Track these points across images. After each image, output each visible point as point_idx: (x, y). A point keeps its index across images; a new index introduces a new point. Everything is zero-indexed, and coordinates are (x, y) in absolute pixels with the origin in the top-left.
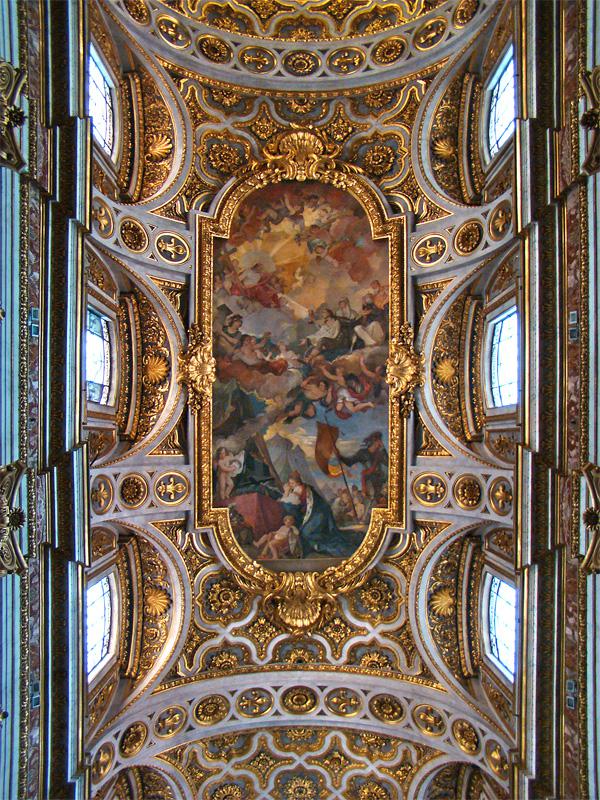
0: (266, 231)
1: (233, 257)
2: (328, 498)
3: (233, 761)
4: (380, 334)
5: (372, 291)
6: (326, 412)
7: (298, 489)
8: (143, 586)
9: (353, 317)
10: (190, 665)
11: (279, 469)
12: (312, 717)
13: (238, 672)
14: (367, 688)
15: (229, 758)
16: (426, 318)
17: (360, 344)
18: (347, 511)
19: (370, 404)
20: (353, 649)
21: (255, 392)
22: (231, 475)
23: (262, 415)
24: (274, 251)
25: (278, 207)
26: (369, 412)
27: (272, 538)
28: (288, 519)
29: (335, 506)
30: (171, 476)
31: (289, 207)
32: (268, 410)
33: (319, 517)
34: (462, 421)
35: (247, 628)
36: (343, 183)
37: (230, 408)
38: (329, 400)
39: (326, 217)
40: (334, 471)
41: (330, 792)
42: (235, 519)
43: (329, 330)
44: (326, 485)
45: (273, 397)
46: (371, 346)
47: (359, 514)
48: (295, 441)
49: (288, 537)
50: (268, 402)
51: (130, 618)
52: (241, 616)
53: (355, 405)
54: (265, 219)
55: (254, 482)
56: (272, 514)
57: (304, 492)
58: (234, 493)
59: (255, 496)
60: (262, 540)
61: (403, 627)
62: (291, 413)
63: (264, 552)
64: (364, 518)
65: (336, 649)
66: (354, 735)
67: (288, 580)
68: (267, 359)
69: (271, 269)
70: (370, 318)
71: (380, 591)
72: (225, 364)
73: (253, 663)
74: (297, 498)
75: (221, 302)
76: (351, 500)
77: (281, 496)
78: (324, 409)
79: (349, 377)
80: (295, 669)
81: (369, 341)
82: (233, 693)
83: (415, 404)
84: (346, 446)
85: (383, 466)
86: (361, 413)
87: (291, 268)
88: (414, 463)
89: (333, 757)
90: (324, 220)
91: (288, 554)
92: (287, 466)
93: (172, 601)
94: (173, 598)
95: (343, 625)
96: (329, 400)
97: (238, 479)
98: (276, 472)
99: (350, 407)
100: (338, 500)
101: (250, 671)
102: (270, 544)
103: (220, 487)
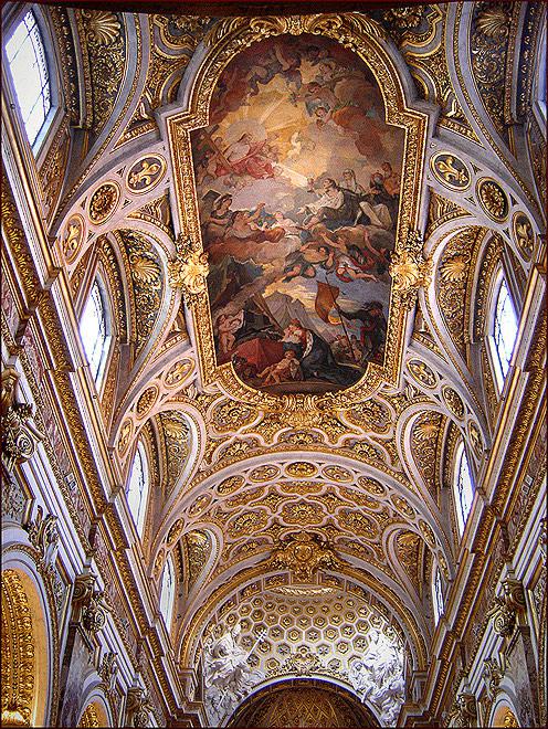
0: (252, 94)
1: (214, 137)
2: (327, 340)
4: (388, 219)
5: (383, 173)
7: (300, 332)
9: (358, 191)
16: (439, 231)
17: (365, 220)
24: (265, 116)
25: (267, 63)
28: (288, 354)
31: (282, 61)
33: (319, 353)
36: (351, 45)
37: (226, 281)
38: (330, 263)
39: (329, 74)
43: (334, 200)
45: (271, 261)
46: (378, 227)
48: (295, 297)
51: (155, 443)
54: (251, 80)
55: (254, 330)
56: (273, 349)
57: (304, 334)
58: (235, 347)
61: (391, 440)
62: (290, 274)
65: (333, 438)
67: (289, 402)
68: (262, 229)
69: (259, 137)
70: (378, 199)
71: (376, 415)
72: (216, 247)
75: (206, 191)
78: (325, 271)
79: (350, 248)
81: (375, 220)
82: (246, 472)
83: (417, 301)
87: (287, 133)
90: (327, 78)
91: (290, 378)
92: (287, 317)
96: (330, 263)
97: (238, 334)
98: (274, 319)
99: (352, 273)
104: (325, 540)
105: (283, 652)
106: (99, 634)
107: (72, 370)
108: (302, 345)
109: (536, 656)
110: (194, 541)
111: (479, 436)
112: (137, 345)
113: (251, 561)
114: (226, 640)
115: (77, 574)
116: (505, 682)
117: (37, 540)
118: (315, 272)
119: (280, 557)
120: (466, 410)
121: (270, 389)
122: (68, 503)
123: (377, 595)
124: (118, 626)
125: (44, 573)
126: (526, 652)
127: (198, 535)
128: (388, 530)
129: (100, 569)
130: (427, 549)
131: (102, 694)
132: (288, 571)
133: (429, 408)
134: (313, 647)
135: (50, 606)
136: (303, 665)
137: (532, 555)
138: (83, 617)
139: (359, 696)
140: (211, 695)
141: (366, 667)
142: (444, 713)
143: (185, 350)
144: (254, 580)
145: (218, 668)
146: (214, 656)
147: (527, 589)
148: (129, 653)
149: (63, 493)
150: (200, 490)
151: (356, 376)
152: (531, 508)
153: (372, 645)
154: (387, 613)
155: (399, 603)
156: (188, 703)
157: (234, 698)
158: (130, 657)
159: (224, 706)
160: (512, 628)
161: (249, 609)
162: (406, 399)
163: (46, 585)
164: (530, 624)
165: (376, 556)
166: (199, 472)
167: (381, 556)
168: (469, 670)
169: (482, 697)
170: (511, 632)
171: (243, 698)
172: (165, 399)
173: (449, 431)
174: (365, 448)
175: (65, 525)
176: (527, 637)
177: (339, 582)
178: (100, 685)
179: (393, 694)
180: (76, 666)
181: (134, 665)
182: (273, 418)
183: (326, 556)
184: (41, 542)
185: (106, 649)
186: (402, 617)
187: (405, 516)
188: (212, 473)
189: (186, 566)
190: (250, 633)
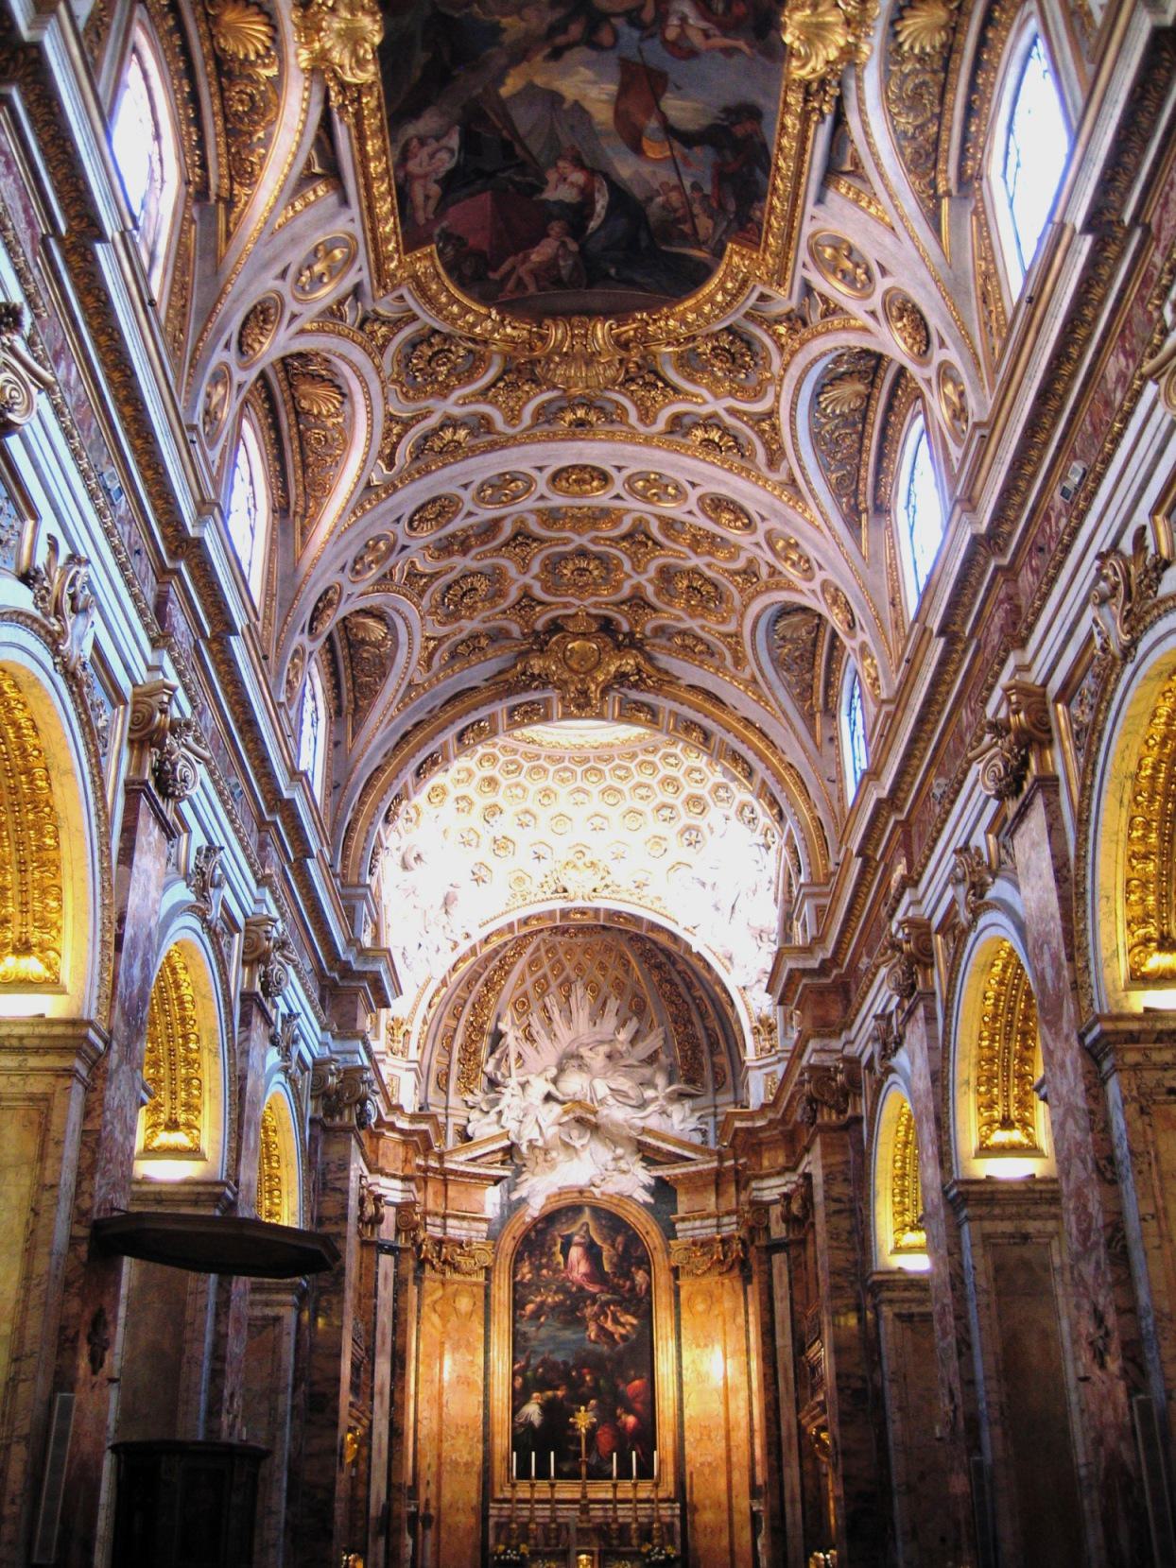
2: (638, 193)
3: (473, 553)
6: (641, 40)
7: (578, 177)
8: (287, 372)
10: (390, 465)
11: (535, 145)
12: (601, 499)
13: (473, 452)
14: (696, 481)
15: (465, 552)
18: (678, 221)
19: (742, 44)
20: (676, 420)
21: (476, 8)
22: (434, 177)
23: (493, 50)
26: (736, 59)
27: (526, 259)
28: (556, 227)
29: (654, 210)
30: (316, 250)
32: (507, 38)
34: (938, 133)
35: (488, 389)
37: (421, 57)
40: (654, 150)
41: (629, 576)
42: (449, 249)
44: (637, 172)
47: (702, 232)
49: (556, 257)
50: (505, 22)
51: (276, 426)
52: (469, 376)
53: (707, 35)
57: (589, 183)
59: (486, 198)
60: (505, 267)
61: (771, 414)
62: (560, 40)
63: (510, 285)
64: (711, 243)
65: (646, 416)
66: (668, 524)
67: (556, 333)
73: (499, 433)
74: (575, 192)
76: (688, 203)
77: (541, 191)
78: (636, 34)
80: (572, 437)
83: (840, 101)
84: (683, 109)
85: (758, 172)
86: (720, 56)
88: (820, 200)
89: (638, 538)
91: (558, 282)
93: (343, 395)
94: (345, 390)
95: (660, 384)
96: (648, 14)
97: (452, 183)
98: (525, 148)
99: (696, 39)
100: (660, 200)
101: (492, 447)
102: (522, 271)
103: (414, 209)
104: (625, 627)
106: (185, 806)
107: (102, 237)
108: (581, 210)
109: (1071, 835)
110: (361, 635)
111: (961, 394)
112: (230, 203)
113: (477, 673)
115: (135, 685)
116: (999, 889)
117: (50, 607)
118: (616, 36)
119: (537, 665)
120: (935, 340)
121: (512, 307)
122: (108, 533)
123: (730, 738)
124: (220, 793)
125: (70, 675)
126: (1051, 828)
127: (371, 622)
128: (755, 607)
129: (180, 674)
130: (834, 635)
131: (196, 924)
132: (553, 694)
133: (856, 341)
135: (86, 744)
137: (1070, 633)
138: (154, 770)
142: (865, 959)
143: (333, 217)
144: (484, 712)
146: (405, 866)
147: (1056, 700)
148: (244, 849)
149: (100, 513)
150: (372, 524)
151: (690, 277)
152: (1074, 533)
154: (750, 773)
155: (774, 753)
158: (248, 857)
160: (1019, 779)
161: (470, 774)
162: (805, 324)
163: (74, 701)
164: (1060, 771)
165: (729, 661)
166: (369, 486)
167: (738, 661)
168: (920, 875)
169: (948, 926)
170: (1020, 788)
171: (465, 947)
172: (295, 327)
173: (892, 395)
174: (715, 435)
175: (103, 576)
176: (1052, 797)
177: (653, 712)
178: (192, 909)
180: (148, 862)
181: (255, 874)
182: (522, 371)
183: (629, 663)
184: (58, 611)
185: (199, 840)
186: (780, 780)
187: (792, 574)
188: (395, 488)
189: (346, 685)
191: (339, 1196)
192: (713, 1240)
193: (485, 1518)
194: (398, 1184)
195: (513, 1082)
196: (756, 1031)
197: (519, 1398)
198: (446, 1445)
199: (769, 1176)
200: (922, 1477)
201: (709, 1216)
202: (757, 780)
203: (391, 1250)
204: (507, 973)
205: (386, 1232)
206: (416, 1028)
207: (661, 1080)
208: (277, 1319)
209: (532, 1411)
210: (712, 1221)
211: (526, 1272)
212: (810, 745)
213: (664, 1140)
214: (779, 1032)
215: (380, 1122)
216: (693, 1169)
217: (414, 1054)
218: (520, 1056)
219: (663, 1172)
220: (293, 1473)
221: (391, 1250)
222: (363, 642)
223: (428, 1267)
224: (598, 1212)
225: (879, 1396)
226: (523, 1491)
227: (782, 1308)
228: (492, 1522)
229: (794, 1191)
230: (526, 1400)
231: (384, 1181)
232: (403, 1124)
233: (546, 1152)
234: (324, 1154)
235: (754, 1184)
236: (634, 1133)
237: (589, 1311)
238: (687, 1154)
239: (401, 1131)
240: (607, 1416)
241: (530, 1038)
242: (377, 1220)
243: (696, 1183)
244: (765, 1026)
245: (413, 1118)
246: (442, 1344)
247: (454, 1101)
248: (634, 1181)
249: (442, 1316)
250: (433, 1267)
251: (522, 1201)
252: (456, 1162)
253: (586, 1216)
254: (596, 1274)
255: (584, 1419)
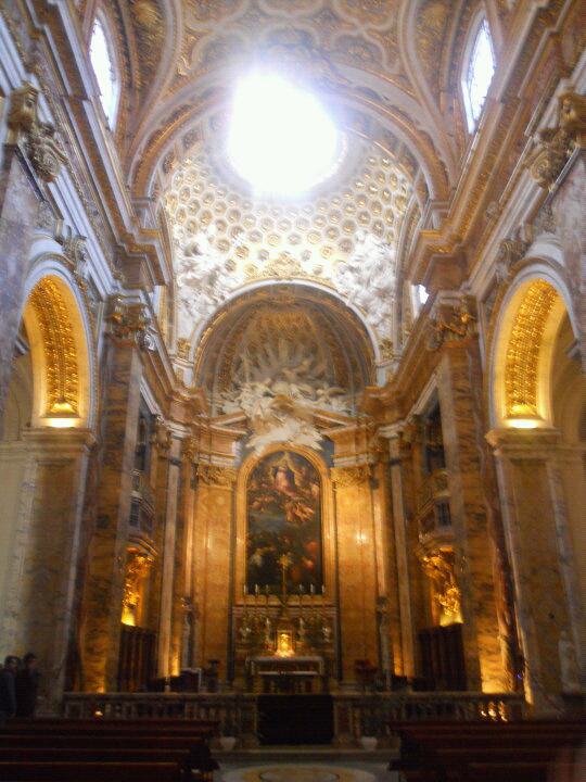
105: (262, 258)
114: (200, 239)
134: (295, 253)
136: (284, 271)
139: (343, 299)
140: (185, 297)
141: (352, 269)
145: (190, 268)
146: (187, 254)
153: (359, 249)
156: (142, 231)
157: (211, 302)
159: (200, 310)
171: (221, 302)
179: (382, 294)
186: (415, 142)
189: (135, 65)
190: (226, 236)
191: (124, 387)
192: (355, 467)
193: (230, 615)
194: (182, 428)
195: (247, 385)
196: (382, 348)
197: (250, 551)
198: (209, 575)
199: (389, 424)
200: (534, 572)
201: (351, 455)
202: (399, 149)
203: (177, 463)
204: (245, 328)
205: (176, 448)
206: (193, 345)
207: (326, 385)
208: (72, 461)
209: (257, 558)
210: (354, 458)
211: (254, 485)
212: (437, 112)
213: (328, 416)
214: (395, 345)
215: (172, 392)
216: (343, 430)
217: (191, 359)
218: (252, 376)
219: (328, 432)
220: (81, 569)
221: (177, 463)
222: (145, 30)
223: (200, 481)
224: (293, 455)
225: (498, 517)
226: (251, 601)
227: (398, 496)
228: (234, 619)
229: (405, 429)
230: (254, 553)
231: (174, 425)
232: (185, 395)
233: (265, 422)
234: (114, 359)
235: (380, 429)
236: (312, 413)
237: (288, 505)
238: (339, 422)
239: (183, 398)
240: (297, 561)
241: (257, 365)
242: (166, 446)
243: (344, 439)
244: (387, 344)
245: (191, 392)
246: (208, 521)
247: (216, 395)
248: (311, 439)
249: (209, 507)
250: (203, 480)
251: (253, 449)
252: (217, 426)
253: (286, 457)
254: (292, 487)
255: (285, 561)
